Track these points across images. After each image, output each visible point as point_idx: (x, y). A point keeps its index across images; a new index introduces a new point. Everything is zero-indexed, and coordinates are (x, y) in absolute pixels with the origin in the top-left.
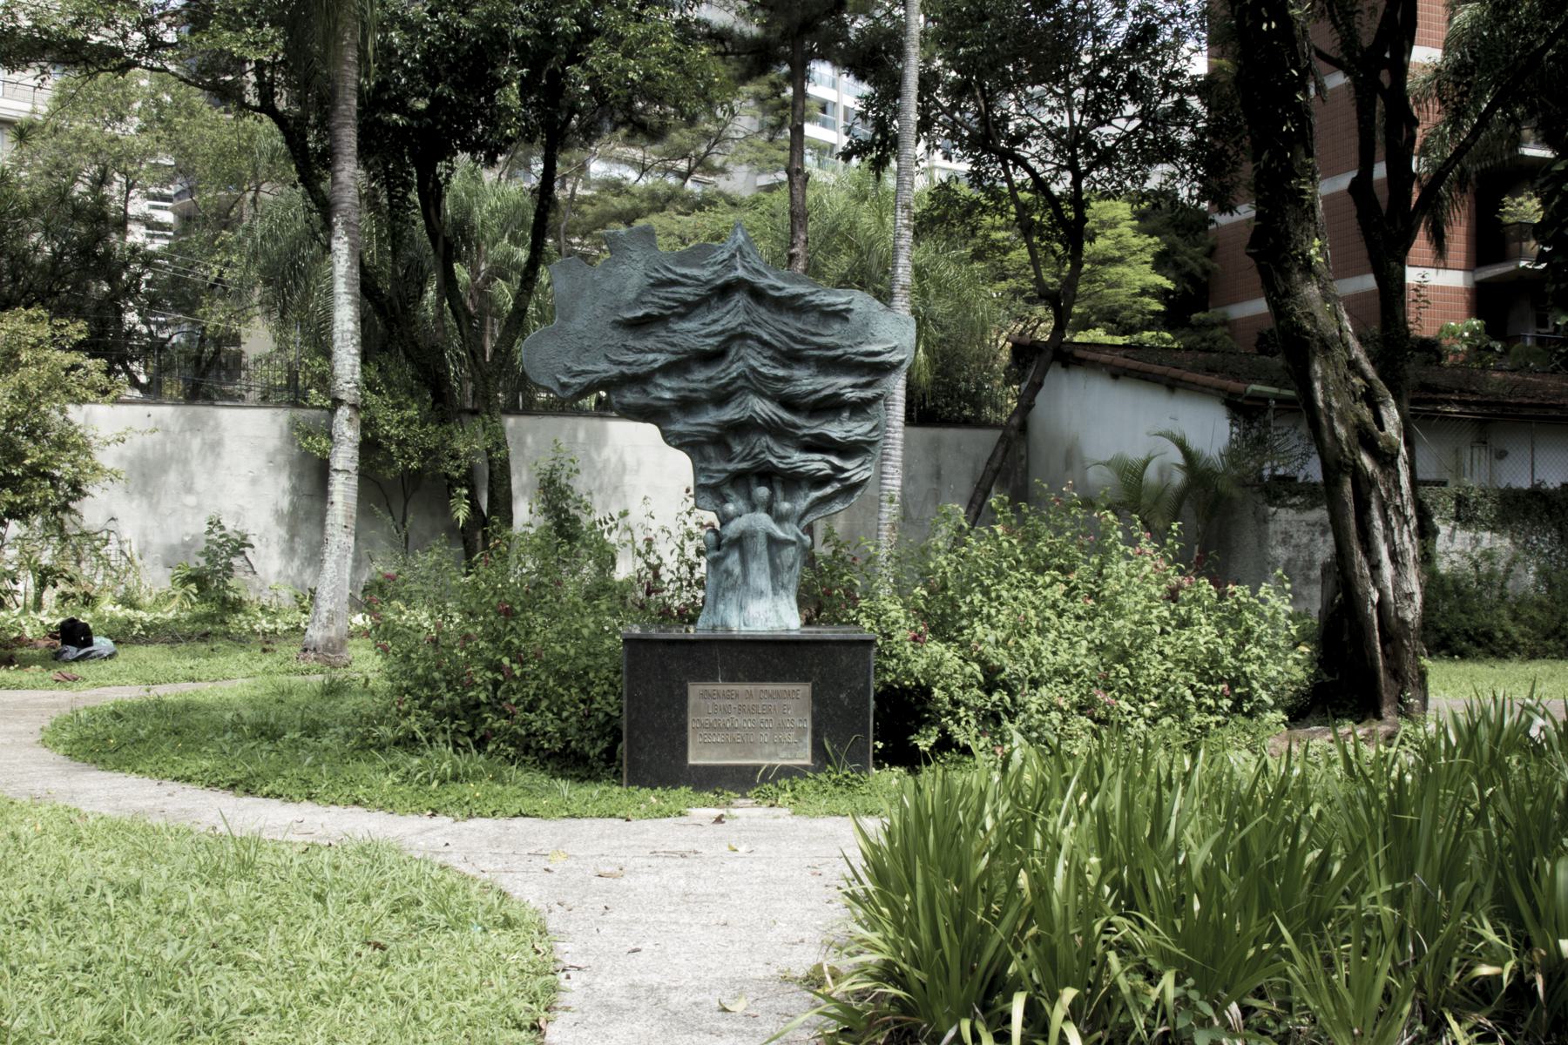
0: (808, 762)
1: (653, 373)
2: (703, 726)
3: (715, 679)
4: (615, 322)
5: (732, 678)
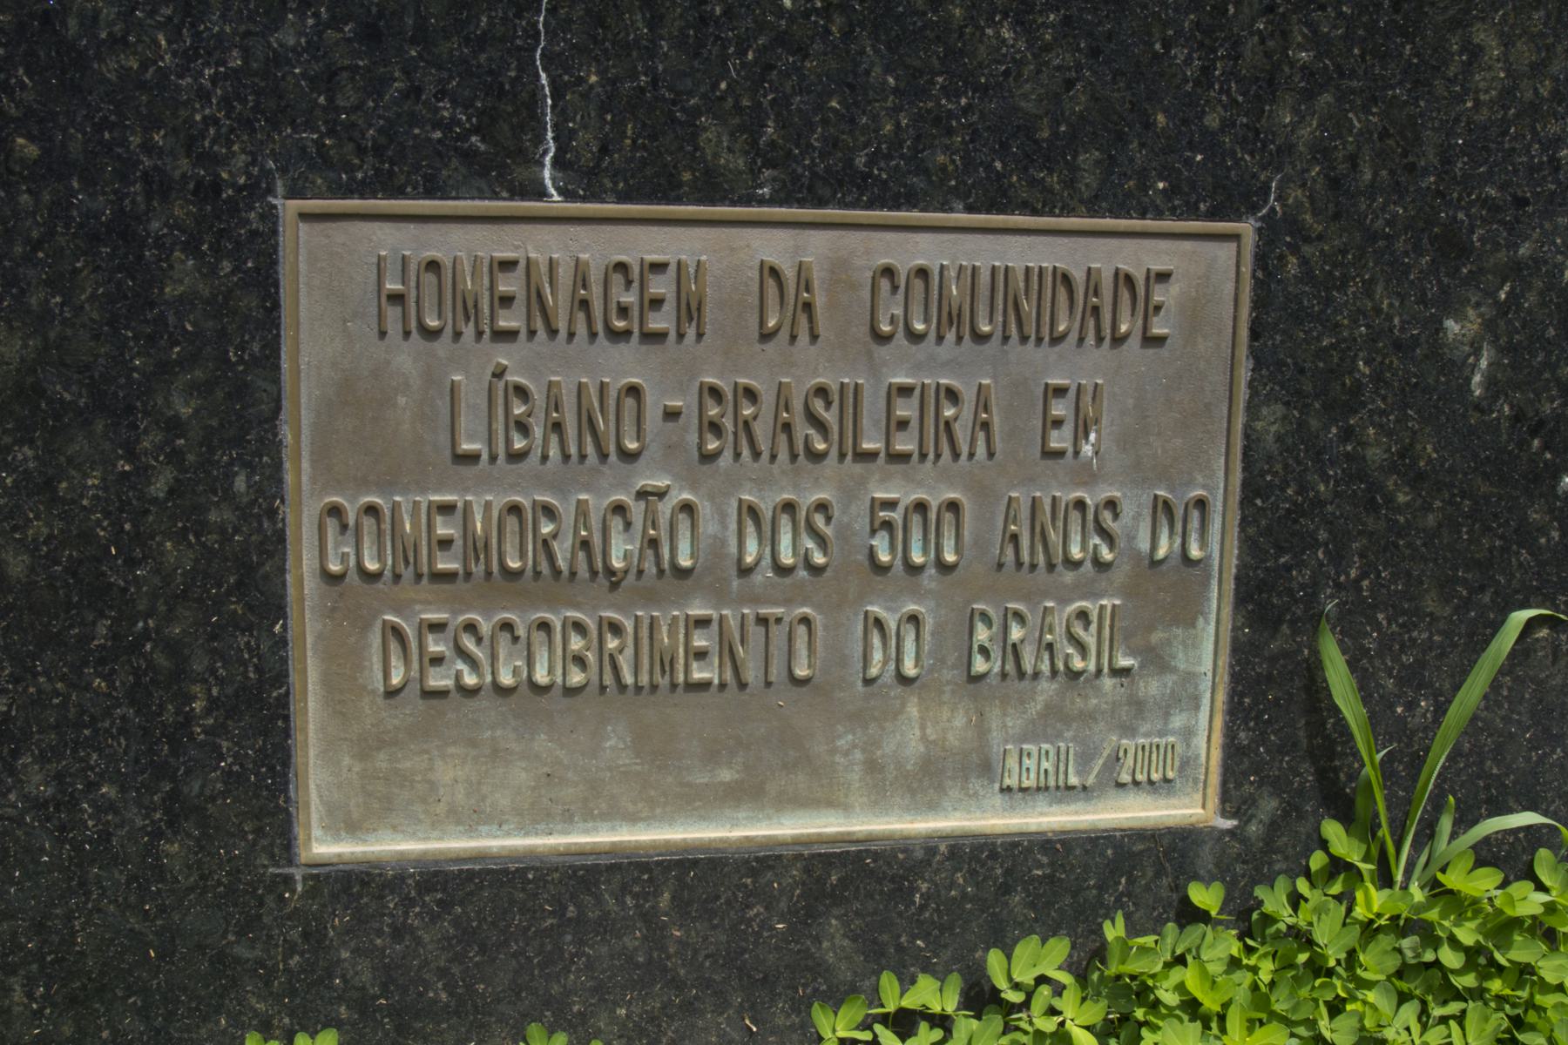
0: (1191, 808)
2: (414, 569)
3: (499, 169)
5: (648, 164)
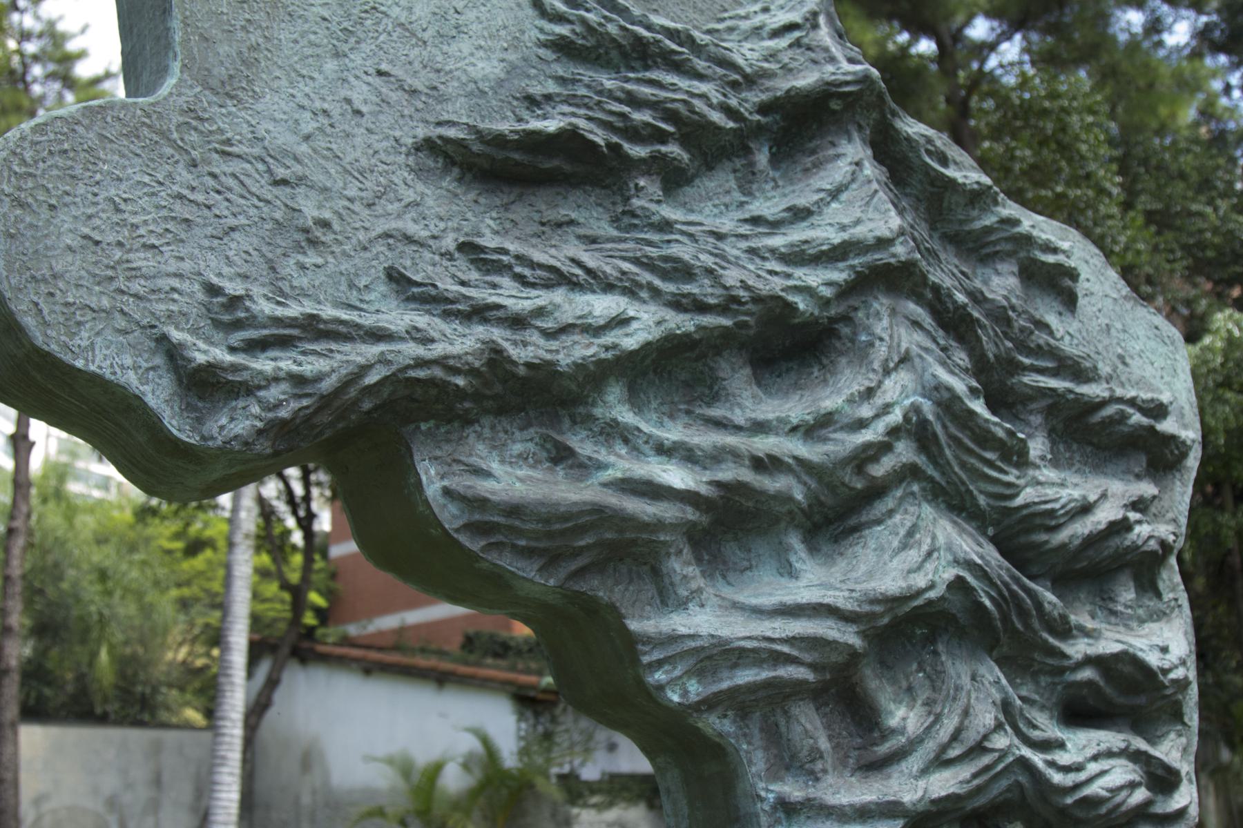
1: (595, 376)
4: (429, 146)
